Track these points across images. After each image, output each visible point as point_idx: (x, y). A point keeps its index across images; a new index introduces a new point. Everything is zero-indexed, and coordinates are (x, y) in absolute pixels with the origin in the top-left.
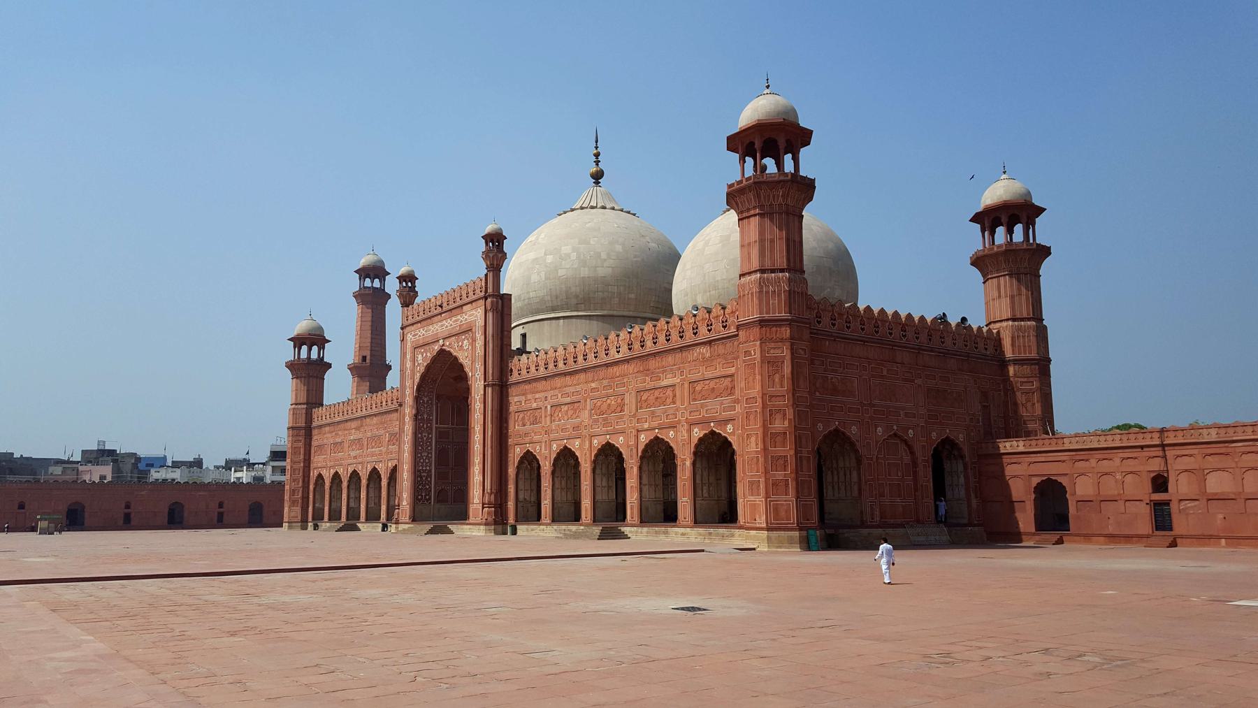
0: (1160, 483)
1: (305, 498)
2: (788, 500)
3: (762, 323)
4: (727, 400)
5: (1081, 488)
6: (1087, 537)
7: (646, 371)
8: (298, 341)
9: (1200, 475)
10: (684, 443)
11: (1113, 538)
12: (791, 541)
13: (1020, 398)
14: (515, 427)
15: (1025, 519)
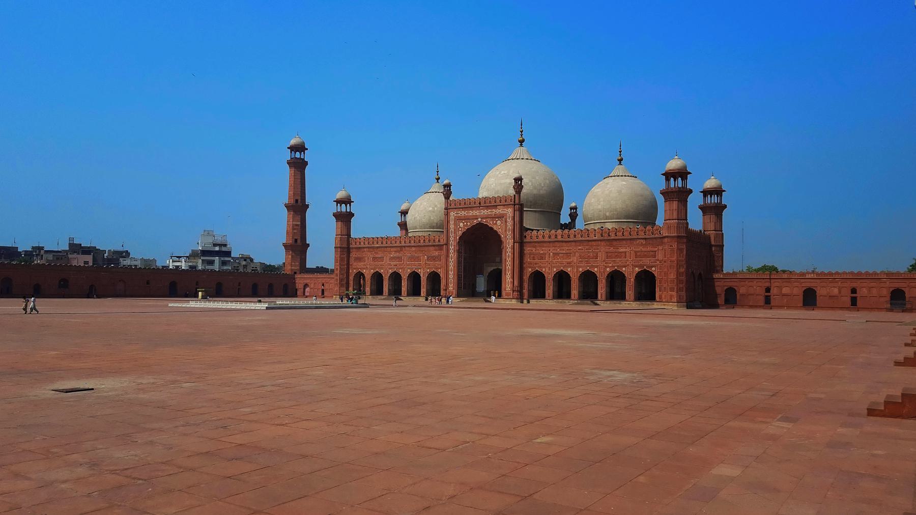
0: (768, 290)
1: (348, 283)
2: (684, 293)
3: (678, 237)
4: (653, 259)
5: (742, 290)
6: (743, 306)
7: (611, 245)
8: (339, 202)
9: (780, 288)
10: (630, 273)
11: (751, 307)
12: (683, 306)
13: (716, 259)
14: (527, 259)
15: (721, 300)
